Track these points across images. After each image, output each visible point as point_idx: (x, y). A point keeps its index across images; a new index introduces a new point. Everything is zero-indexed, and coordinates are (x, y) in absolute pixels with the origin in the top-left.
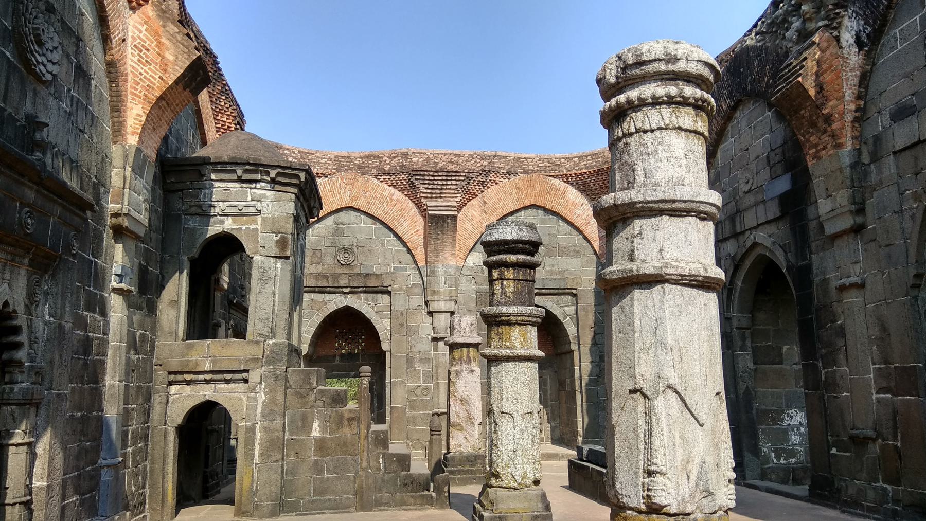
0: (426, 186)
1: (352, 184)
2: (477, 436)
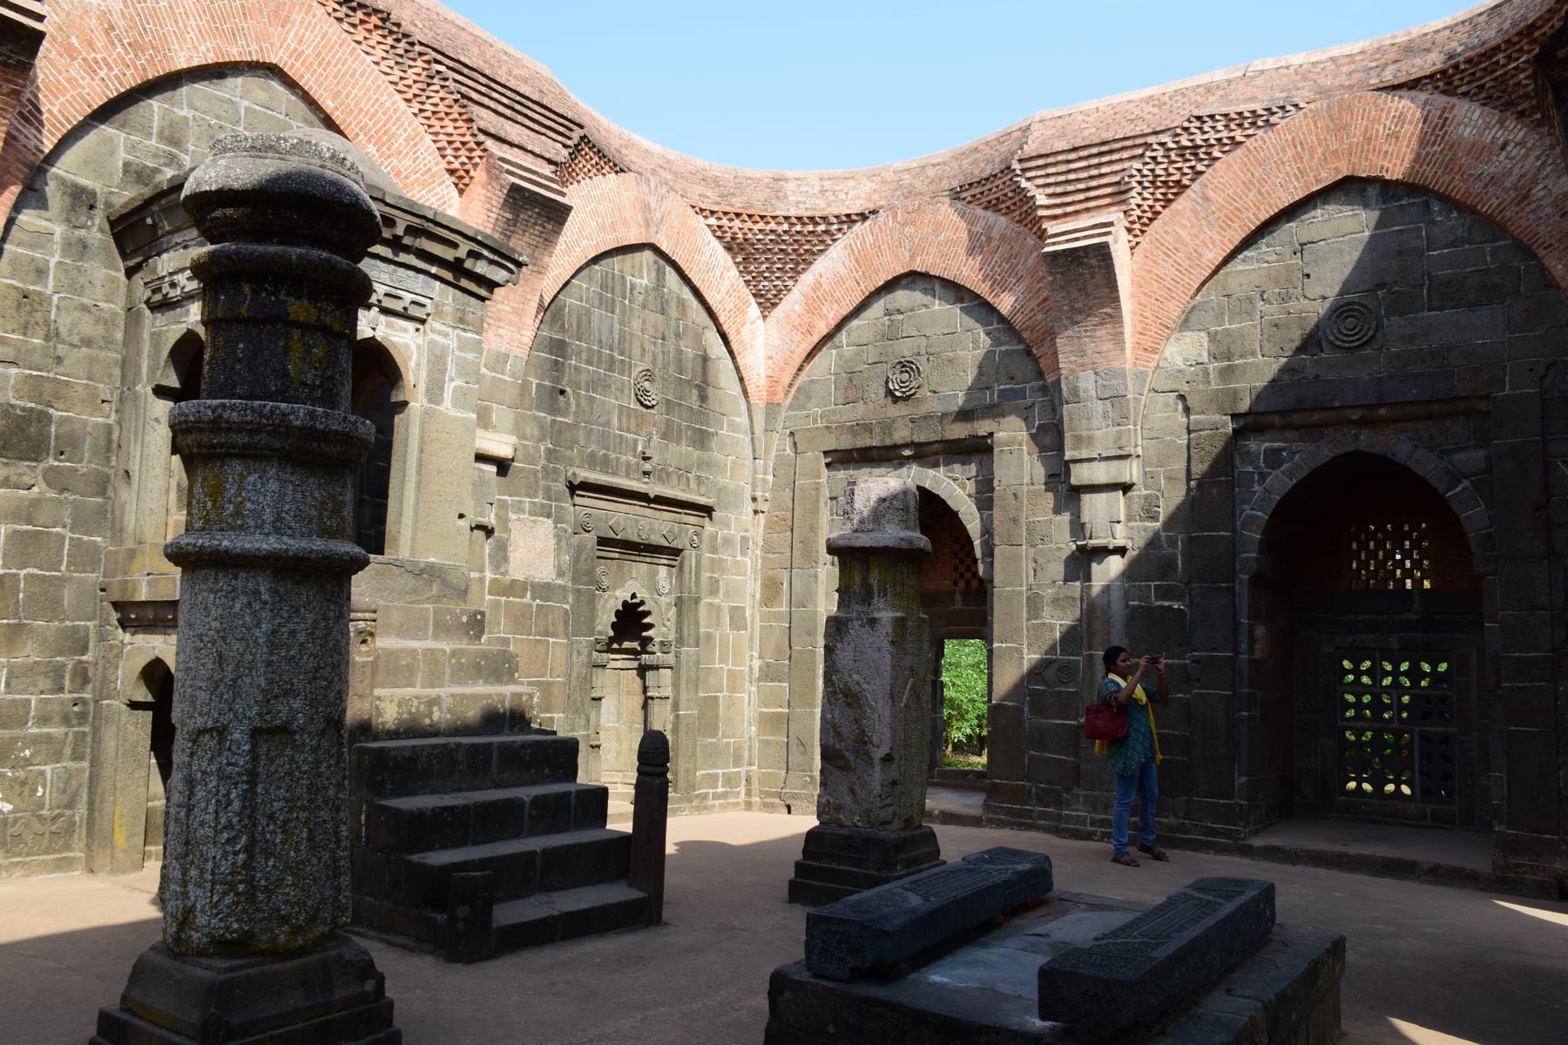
0: (1050, 190)
1: (913, 223)
2: (877, 789)
